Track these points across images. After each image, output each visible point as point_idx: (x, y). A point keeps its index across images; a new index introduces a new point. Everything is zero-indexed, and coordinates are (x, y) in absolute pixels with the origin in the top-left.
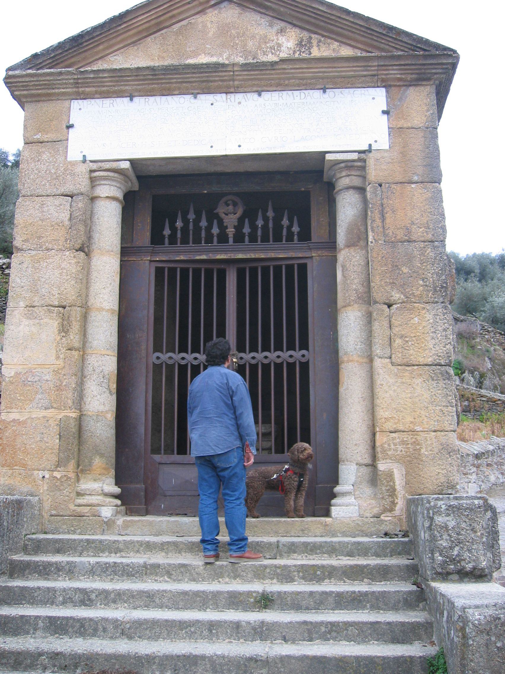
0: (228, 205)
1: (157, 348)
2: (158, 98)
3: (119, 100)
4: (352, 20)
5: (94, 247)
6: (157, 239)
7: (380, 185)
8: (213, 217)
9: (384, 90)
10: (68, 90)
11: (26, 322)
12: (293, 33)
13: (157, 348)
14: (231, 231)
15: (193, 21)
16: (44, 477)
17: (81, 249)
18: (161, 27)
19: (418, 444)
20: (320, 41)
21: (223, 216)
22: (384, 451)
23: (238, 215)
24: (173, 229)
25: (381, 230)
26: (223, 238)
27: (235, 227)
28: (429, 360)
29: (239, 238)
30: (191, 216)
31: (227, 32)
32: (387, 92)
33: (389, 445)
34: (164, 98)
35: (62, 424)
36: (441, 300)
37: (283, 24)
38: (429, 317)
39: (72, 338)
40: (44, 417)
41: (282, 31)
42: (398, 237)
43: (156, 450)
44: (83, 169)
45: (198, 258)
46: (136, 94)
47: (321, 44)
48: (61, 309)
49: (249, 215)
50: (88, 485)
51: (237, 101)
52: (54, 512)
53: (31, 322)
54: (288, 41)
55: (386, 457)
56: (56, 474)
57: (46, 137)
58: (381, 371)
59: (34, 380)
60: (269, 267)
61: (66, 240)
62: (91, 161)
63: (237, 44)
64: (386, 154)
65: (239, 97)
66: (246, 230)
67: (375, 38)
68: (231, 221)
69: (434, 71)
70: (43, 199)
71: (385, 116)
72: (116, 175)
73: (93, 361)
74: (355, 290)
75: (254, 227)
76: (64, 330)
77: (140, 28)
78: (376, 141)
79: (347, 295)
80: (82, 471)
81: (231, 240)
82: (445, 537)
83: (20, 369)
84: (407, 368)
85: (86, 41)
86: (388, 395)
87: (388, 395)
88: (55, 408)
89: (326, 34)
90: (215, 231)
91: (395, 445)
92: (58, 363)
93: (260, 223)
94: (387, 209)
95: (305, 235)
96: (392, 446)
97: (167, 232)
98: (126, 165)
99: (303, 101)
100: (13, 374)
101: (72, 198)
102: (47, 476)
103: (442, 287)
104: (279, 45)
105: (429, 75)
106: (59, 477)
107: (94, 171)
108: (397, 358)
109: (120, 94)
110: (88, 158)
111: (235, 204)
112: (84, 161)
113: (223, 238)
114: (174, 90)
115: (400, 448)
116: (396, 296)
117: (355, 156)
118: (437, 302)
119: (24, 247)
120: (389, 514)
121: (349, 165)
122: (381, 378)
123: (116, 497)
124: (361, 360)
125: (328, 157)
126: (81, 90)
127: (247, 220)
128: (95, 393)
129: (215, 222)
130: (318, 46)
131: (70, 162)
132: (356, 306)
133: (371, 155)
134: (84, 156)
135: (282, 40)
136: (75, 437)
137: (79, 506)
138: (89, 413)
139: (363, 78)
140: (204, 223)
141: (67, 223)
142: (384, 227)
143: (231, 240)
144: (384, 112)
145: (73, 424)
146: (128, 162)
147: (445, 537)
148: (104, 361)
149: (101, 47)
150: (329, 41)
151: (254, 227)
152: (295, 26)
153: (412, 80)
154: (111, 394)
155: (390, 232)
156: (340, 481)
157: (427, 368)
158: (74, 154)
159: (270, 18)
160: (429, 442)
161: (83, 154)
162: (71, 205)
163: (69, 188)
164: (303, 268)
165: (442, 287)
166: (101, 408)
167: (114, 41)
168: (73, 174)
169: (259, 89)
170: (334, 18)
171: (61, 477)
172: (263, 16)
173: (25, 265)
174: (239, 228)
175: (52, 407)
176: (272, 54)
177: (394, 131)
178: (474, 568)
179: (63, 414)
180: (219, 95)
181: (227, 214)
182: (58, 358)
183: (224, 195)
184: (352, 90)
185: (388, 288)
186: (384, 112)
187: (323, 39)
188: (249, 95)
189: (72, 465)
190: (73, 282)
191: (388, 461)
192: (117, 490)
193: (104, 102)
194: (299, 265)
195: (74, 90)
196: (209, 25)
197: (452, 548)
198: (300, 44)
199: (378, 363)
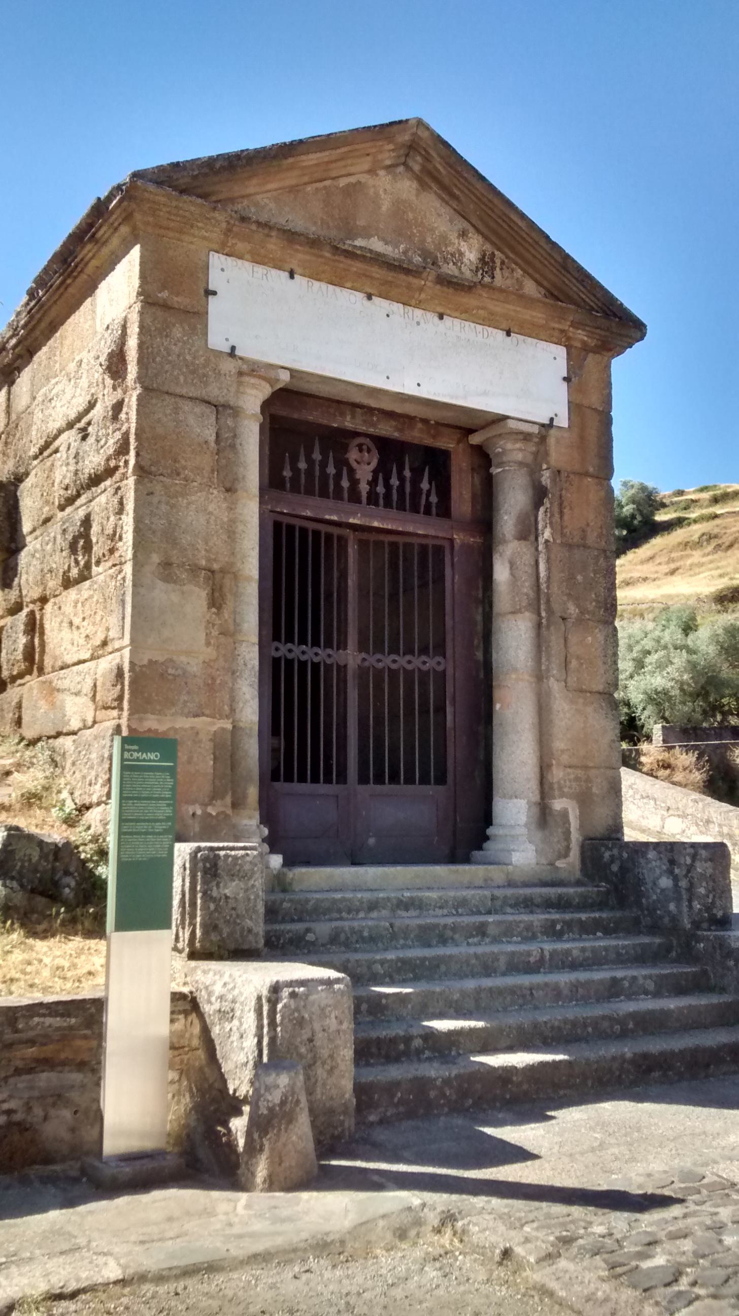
2: (324, 286)
3: (274, 272)
4: (549, 251)
8: (342, 463)
12: (476, 241)
14: (364, 488)
15: (363, 180)
16: (194, 814)
20: (503, 263)
21: (354, 465)
24: (295, 470)
26: (354, 497)
27: (369, 483)
30: (317, 456)
31: (404, 212)
34: (331, 287)
37: (466, 225)
39: (227, 617)
40: (192, 728)
41: (463, 234)
42: (575, 540)
44: (228, 366)
45: (327, 517)
49: (382, 470)
51: (416, 320)
53: (170, 586)
58: (557, 695)
59: (177, 673)
60: (412, 545)
61: (213, 471)
62: (241, 358)
65: (418, 312)
67: (567, 282)
68: (364, 473)
70: (178, 399)
74: (526, 594)
75: (388, 486)
79: (517, 599)
82: (704, 884)
86: (563, 723)
87: (563, 723)
88: (207, 716)
89: (511, 255)
90: (345, 484)
91: (570, 781)
92: (209, 650)
94: (566, 503)
95: (444, 511)
100: (145, 662)
101: (215, 406)
102: (199, 812)
104: (461, 254)
106: (214, 814)
108: (572, 680)
113: (354, 497)
115: (574, 784)
116: (573, 610)
117: (535, 429)
119: (153, 469)
120: (564, 861)
122: (557, 702)
125: (511, 424)
127: (381, 475)
130: (501, 269)
132: (527, 614)
133: (553, 432)
135: (464, 247)
140: (331, 470)
146: (288, 373)
150: (514, 266)
151: (388, 486)
155: (567, 531)
156: (494, 822)
159: (452, 211)
161: (232, 342)
162: (217, 419)
164: (439, 551)
170: (530, 241)
171: (218, 814)
173: (155, 500)
174: (373, 483)
175: (203, 715)
176: (454, 264)
177: (575, 408)
181: (358, 463)
182: (208, 644)
183: (356, 434)
185: (565, 598)
187: (506, 261)
193: (255, 269)
199: (555, 685)
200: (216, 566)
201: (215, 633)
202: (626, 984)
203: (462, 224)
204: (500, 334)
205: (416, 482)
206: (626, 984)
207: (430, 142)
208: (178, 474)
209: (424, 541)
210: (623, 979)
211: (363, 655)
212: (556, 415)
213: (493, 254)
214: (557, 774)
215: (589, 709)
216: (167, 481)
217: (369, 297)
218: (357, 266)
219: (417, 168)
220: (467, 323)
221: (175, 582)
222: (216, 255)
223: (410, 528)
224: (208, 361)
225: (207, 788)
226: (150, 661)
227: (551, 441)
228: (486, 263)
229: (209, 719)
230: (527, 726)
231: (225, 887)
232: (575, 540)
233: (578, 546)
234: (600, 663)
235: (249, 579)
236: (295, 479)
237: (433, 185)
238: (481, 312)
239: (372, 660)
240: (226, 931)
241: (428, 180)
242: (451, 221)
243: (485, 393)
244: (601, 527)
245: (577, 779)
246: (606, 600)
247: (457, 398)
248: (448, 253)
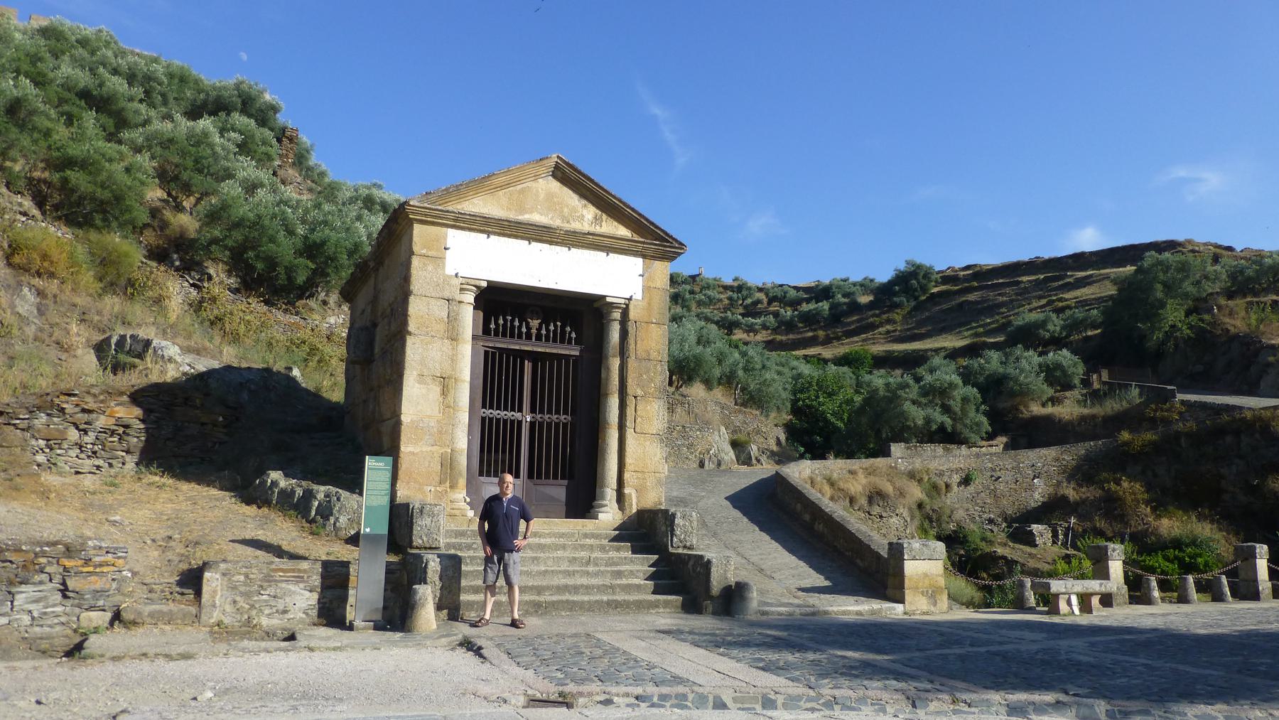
1: (484, 406)
6: (486, 331)
13: (484, 406)
14: (534, 331)
26: (529, 337)
29: (539, 337)
35: (442, 456)
43: (481, 474)
44: (457, 282)
57: (430, 253)
66: (544, 332)
68: (535, 323)
75: (548, 330)
76: (444, 393)
83: (415, 418)
90: (524, 330)
93: (552, 328)
97: (493, 326)
113: (529, 337)
116: (639, 392)
117: (623, 301)
125: (608, 299)
135: (585, 212)
136: (448, 464)
140: (517, 323)
151: (548, 330)
158: (450, 270)
163: (447, 294)
174: (539, 329)
177: (646, 289)
198: (595, 218)
203: (584, 202)
205: (563, 327)
214: (627, 476)
225: (437, 479)
227: (631, 307)
235: (464, 381)
236: (496, 331)
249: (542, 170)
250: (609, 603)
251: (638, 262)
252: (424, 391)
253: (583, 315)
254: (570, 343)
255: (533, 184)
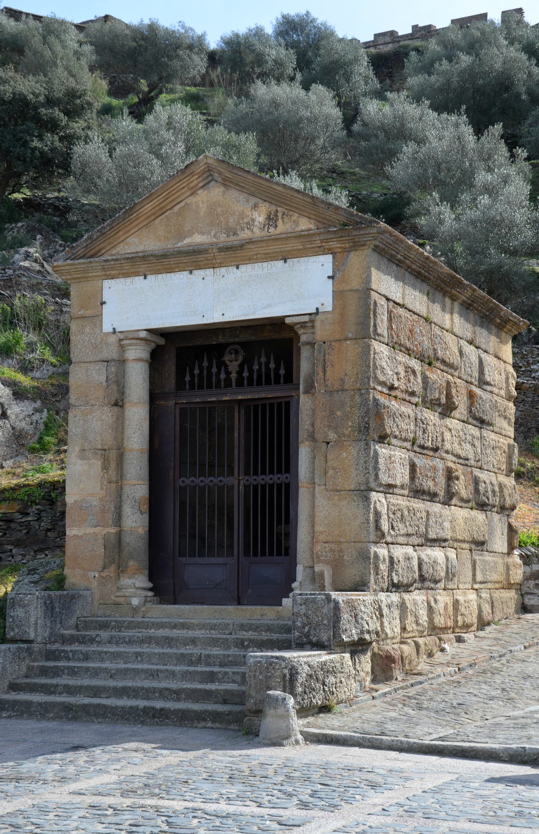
0: (231, 354)
2: (164, 275)
3: (137, 278)
5: (126, 401)
6: (180, 385)
7: (324, 343)
8: (221, 364)
9: (331, 256)
10: (99, 274)
11: (80, 462)
14: (234, 376)
15: (189, 202)
17: (116, 404)
18: (164, 210)
19: (342, 552)
21: (228, 363)
22: (318, 557)
23: (239, 362)
24: (192, 375)
25: (323, 381)
26: (228, 383)
28: (352, 487)
30: (205, 364)
31: (215, 210)
32: (334, 258)
33: (322, 552)
34: (169, 275)
35: (106, 538)
36: (364, 437)
38: (354, 452)
40: (94, 533)
41: (255, 207)
42: (335, 388)
43: (182, 554)
44: (113, 339)
45: (209, 400)
46: (148, 273)
47: (285, 216)
48: (103, 452)
49: (247, 362)
50: (126, 581)
51: (222, 274)
52: (101, 602)
53: (84, 462)
54: (260, 216)
55: (319, 561)
56: (102, 574)
61: (105, 398)
62: (120, 332)
63: (221, 222)
64: (329, 316)
65: (223, 270)
66: (246, 374)
68: (233, 367)
69: (365, 239)
71: (331, 281)
72: (139, 341)
73: (128, 490)
74: (307, 430)
75: (251, 371)
76: (105, 468)
77: (148, 215)
78: (323, 304)
80: (122, 572)
81: (234, 384)
82: (300, 619)
84: (336, 493)
85: (108, 231)
86: (322, 514)
87: (322, 514)
90: (223, 376)
91: (326, 552)
92: (102, 492)
93: (256, 367)
94: (328, 364)
96: (324, 554)
97: (187, 378)
98: (143, 334)
99: (270, 271)
100: (73, 502)
102: (97, 576)
103: (365, 427)
104: (253, 220)
105: (363, 243)
107: (123, 340)
109: (137, 274)
110: (118, 330)
111: (237, 352)
112: (114, 331)
114: (175, 268)
115: (329, 554)
116: (332, 436)
118: (361, 440)
121: (303, 325)
123: (151, 590)
124: (309, 486)
125: (288, 321)
126: (108, 273)
127: (246, 366)
128: (129, 513)
129: (223, 367)
130: (283, 218)
131: (104, 334)
132: (307, 443)
133: (318, 317)
134: (114, 329)
135: (255, 215)
136: (116, 548)
137: (118, 597)
138: (126, 529)
139: (312, 250)
140: (214, 370)
141: (104, 384)
142: (325, 379)
143: (234, 384)
144: (329, 277)
145: (112, 538)
147: (300, 619)
148: (137, 488)
149: (121, 233)
150: (291, 213)
151: (251, 371)
152: (265, 201)
153: (351, 247)
154: (142, 513)
155: (329, 383)
157: (351, 492)
158: (107, 328)
159: (246, 195)
160: (350, 550)
163: (106, 355)
165: (365, 427)
166: (134, 525)
167: (130, 227)
168: (107, 344)
169: (237, 263)
172: (241, 193)
174: (240, 373)
175: (99, 526)
176: (248, 229)
177: (337, 295)
178: (318, 641)
179: (106, 531)
180: (208, 270)
181: (231, 361)
182: (102, 489)
183: (229, 344)
184: (306, 259)
186: (329, 277)
188: (230, 268)
189: (113, 568)
190: (110, 431)
191: (321, 564)
192: (151, 585)
194: (285, 402)
195: (103, 273)
196: (201, 205)
197: (304, 628)
198: (269, 218)
200: (106, 447)
201: (105, 483)
202: (220, 676)
203: (253, 200)
204: (280, 263)
206: (220, 676)
207: (216, 164)
208: (88, 404)
209: (263, 402)
210: (219, 672)
211: (247, 477)
212: (323, 304)
213: (277, 211)
215: (344, 503)
216: (83, 408)
217: (191, 273)
218: (173, 261)
219: (220, 179)
220: (256, 265)
221: (86, 459)
222: (106, 281)
223: (263, 395)
224: (102, 340)
225: (101, 563)
226: (75, 501)
227: (318, 324)
228: (272, 220)
229: (102, 528)
230: (305, 517)
231: (17, 611)
232: (335, 388)
233: (338, 391)
234: (353, 470)
236: (192, 382)
237: (231, 185)
238: (259, 256)
239: (254, 480)
240: (17, 631)
241: (227, 183)
242: (247, 201)
243: (269, 306)
244: (357, 374)
245: (331, 550)
246: (359, 424)
247: (248, 315)
248: (244, 223)
249: (195, 180)
250: (146, 711)
251: (323, 265)
252: (86, 467)
253: (270, 347)
254: (277, 382)
255: (192, 200)
